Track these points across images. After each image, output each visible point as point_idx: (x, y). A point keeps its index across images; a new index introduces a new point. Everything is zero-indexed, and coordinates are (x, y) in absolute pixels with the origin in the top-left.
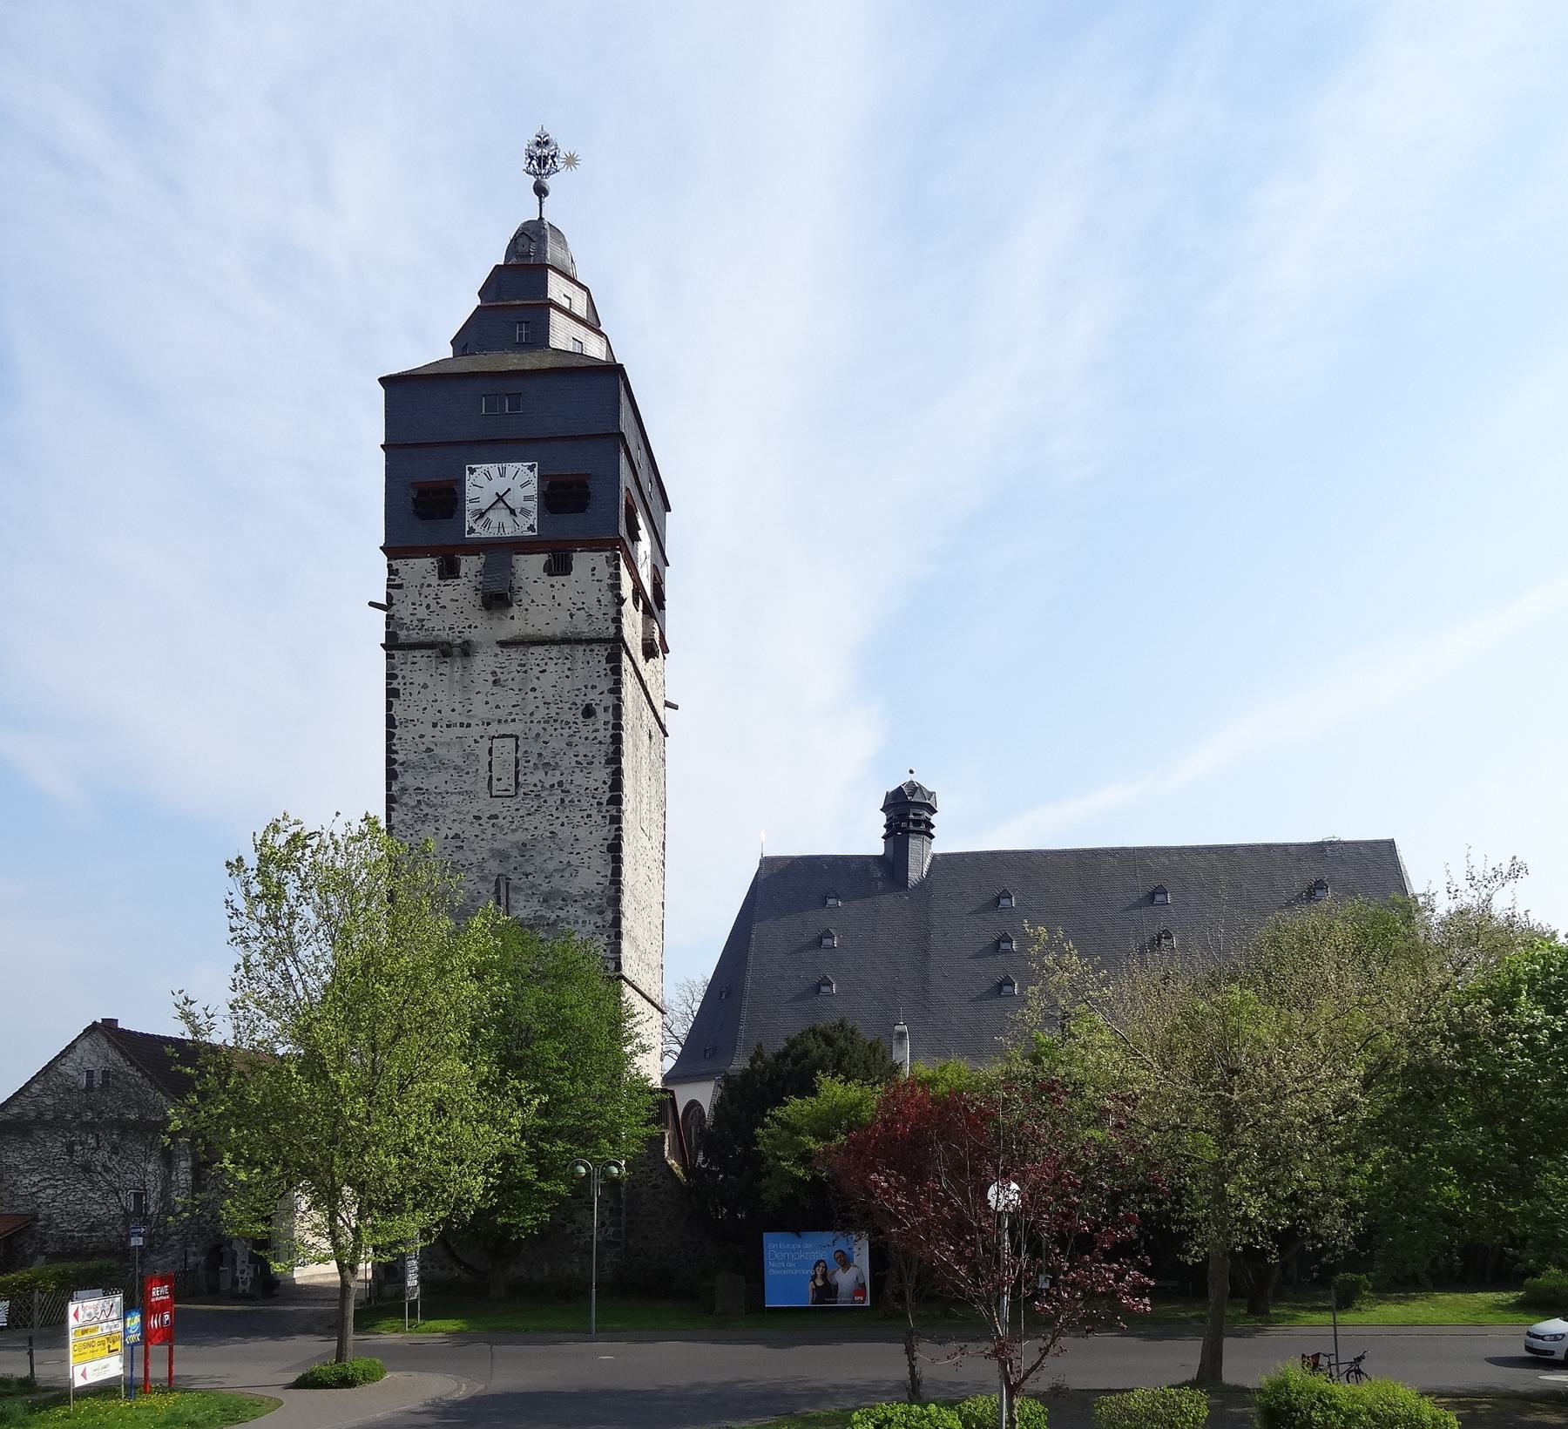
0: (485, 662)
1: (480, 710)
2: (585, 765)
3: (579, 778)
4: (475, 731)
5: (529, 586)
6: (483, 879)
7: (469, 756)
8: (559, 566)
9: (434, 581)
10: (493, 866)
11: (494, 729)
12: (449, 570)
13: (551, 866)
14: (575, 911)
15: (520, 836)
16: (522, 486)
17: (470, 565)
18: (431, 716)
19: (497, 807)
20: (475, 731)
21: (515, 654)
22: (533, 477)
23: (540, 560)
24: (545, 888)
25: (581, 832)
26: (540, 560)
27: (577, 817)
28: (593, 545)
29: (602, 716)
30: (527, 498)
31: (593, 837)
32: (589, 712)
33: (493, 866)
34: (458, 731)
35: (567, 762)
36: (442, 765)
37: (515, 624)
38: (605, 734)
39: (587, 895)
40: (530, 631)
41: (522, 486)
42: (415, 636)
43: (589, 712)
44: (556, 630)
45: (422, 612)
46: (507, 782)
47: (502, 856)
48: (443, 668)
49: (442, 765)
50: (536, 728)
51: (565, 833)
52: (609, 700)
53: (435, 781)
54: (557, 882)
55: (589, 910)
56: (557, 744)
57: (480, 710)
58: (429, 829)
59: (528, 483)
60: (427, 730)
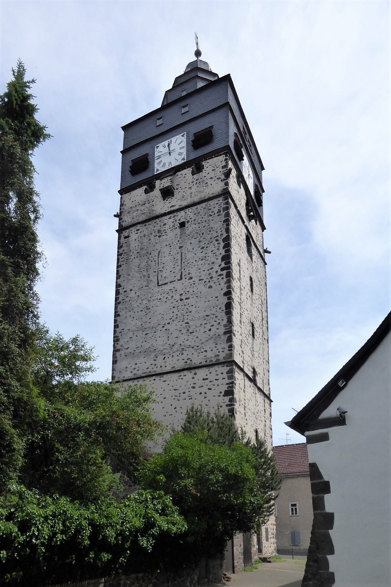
16: (179, 144)
22: (184, 139)
30: (181, 148)
41: (179, 144)
59: (182, 142)
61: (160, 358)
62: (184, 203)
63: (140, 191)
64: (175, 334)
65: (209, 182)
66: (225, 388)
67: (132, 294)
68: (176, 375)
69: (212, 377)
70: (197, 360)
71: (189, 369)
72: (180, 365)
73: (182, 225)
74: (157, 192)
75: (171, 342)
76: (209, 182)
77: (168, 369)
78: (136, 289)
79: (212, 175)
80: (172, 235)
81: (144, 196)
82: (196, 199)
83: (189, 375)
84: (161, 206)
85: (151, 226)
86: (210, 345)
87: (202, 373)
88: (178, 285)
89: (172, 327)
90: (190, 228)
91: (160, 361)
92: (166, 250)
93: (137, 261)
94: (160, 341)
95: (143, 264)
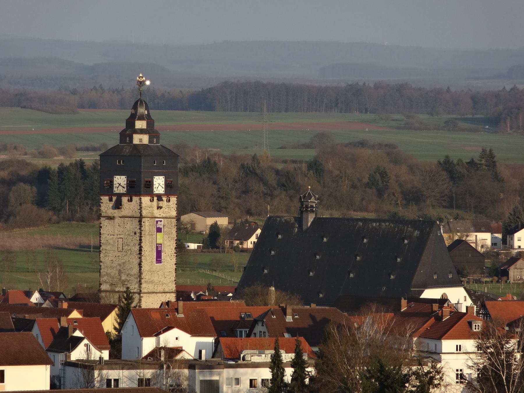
0: (117, 221)
1: (116, 232)
3: (133, 248)
4: (115, 236)
5: (125, 205)
6: (117, 270)
7: (114, 242)
8: (131, 200)
9: (108, 202)
10: (118, 267)
11: (119, 236)
12: (111, 200)
13: (129, 268)
14: (132, 278)
15: (123, 261)
18: (108, 233)
19: (119, 254)
20: (115, 236)
21: (122, 219)
24: (127, 273)
25: (134, 260)
28: (136, 195)
29: (138, 234)
31: (136, 261)
32: (135, 233)
33: (118, 267)
34: (112, 236)
38: (138, 238)
40: (125, 214)
43: (135, 233)
44: (129, 215)
46: (121, 248)
47: (120, 265)
48: (110, 222)
50: (126, 237)
51: (131, 260)
52: (139, 231)
53: (108, 248)
54: (129, 271)
55: (135, 278)
57: (116, 232)
58: (107, 258)
61: (156, 286)
62: (164, 215)
65: (172, 209)
67: (147, 253)
68: (160, 295)
70: (167, 290)
71: (165, 293)
72: (162, 290)
76: (172, 209)
77: (158, 291)
78: (148, 251)
79: (172, 206)
81: (149, 203)
82: (168, 215)
84: (157, 213)
93: (148, 236)
94: (156, 279)
95: (150, 240)
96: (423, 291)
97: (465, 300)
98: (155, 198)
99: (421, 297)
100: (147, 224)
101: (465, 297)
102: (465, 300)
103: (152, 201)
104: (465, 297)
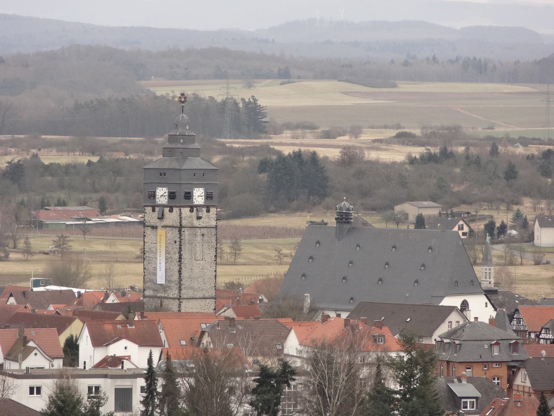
2: (175, 253)
3: (174, 256)
9: (151, 212)
12: (154, 210)
14: (173, 284)
17: (157, 209)
18: (151, 241)
23: (169, 208)
25: (174, 268)
26: (169, 208)
27: (173, 264)
29: (178, 243)
32: (175, 242)
35: (172, 252)
36: (152, 252)
37: (166, 222)
38: (178, 247)
39: (175, 281)
42: (149, 224)
43: (175, 242)
44: (170, 224)
45: (149, 219)
49: (152, 252)
51: (172, 267)
52: (179, 240)
56: (170, 249)
58: (150, 265)
60: (150, 244)
62: (204, 225)
63: (188, 209)
64: (200, 283)
66: (214, 307)
67: (186, 260)
68: (200, 300)
69: (211, 303)
72: (201, 296)
73: (203, 235)
74: (194, 214)
75: (199, 286)
77: (198, 297)
79: (212, 216)
80: (199, 238)
81: (189, 213)
82: (208, 225)
83: (204, 300)
84: (196, 223)
85: (192, 230)
86: (210, 290)
87: (208, 301)
88: (201, 262)
89: (200, 280)
90: (206, 238)
91: (195, 293)
92: (198, 245)
93: (188, 245)
94: (195, 285)
96: (442, 297)
97: (486, 306)
98: (195, 209)
99: (441, 304)
100: (187, 233)
101: (486, 303)
102: (486, 306)
103: (191, 211)
104: (486, 303)
